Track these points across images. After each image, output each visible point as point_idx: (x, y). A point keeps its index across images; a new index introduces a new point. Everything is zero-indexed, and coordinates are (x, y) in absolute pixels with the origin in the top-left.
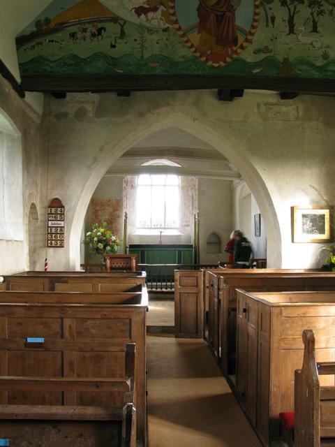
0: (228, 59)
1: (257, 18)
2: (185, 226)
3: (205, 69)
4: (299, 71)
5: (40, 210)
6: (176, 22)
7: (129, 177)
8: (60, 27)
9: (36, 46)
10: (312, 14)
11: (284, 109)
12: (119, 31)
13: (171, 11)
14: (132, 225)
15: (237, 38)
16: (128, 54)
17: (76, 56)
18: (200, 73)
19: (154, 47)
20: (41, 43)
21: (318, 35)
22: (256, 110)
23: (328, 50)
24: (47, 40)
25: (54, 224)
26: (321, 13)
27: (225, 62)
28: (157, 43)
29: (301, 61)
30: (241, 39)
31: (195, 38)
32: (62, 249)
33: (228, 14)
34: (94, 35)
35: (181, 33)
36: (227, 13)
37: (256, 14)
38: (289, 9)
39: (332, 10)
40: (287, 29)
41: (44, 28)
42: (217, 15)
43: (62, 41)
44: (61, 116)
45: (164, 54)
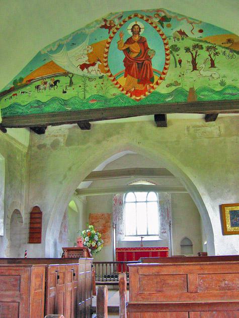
0: (147, 93)
1: (167, 62)
2: (163, 233)
3: (130, 102)
6: (109, 71)
8: (30, 82)
10: (210, 55)
11: (209, 129)
13: (105, 64)
14: (120, 234)
18: (126, 105)
19: (93, 90)
23: (224, 79)
26: (216, 54)
27: (145, 95)
29: (204, 89)
30: (156, 78)
31: (122, 81)
33: (146, 62)
34: (51, 86)
35: (112, 78)
36: (145, 62)
37: (167, 60)
38: (192, 54)
39: (225, 52)
40: (191, 68)
41: (19, 84)
42: (138, 64)
45: (100, 94)
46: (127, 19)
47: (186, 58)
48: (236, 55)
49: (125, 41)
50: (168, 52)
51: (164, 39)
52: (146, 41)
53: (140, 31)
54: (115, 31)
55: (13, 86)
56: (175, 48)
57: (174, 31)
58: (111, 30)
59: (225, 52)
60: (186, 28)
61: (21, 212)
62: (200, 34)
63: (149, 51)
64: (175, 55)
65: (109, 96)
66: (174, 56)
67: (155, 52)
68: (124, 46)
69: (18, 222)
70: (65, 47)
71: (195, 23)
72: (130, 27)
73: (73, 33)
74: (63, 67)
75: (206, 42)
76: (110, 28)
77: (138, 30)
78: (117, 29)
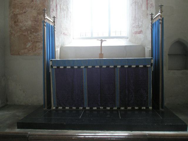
2: (136, 33)
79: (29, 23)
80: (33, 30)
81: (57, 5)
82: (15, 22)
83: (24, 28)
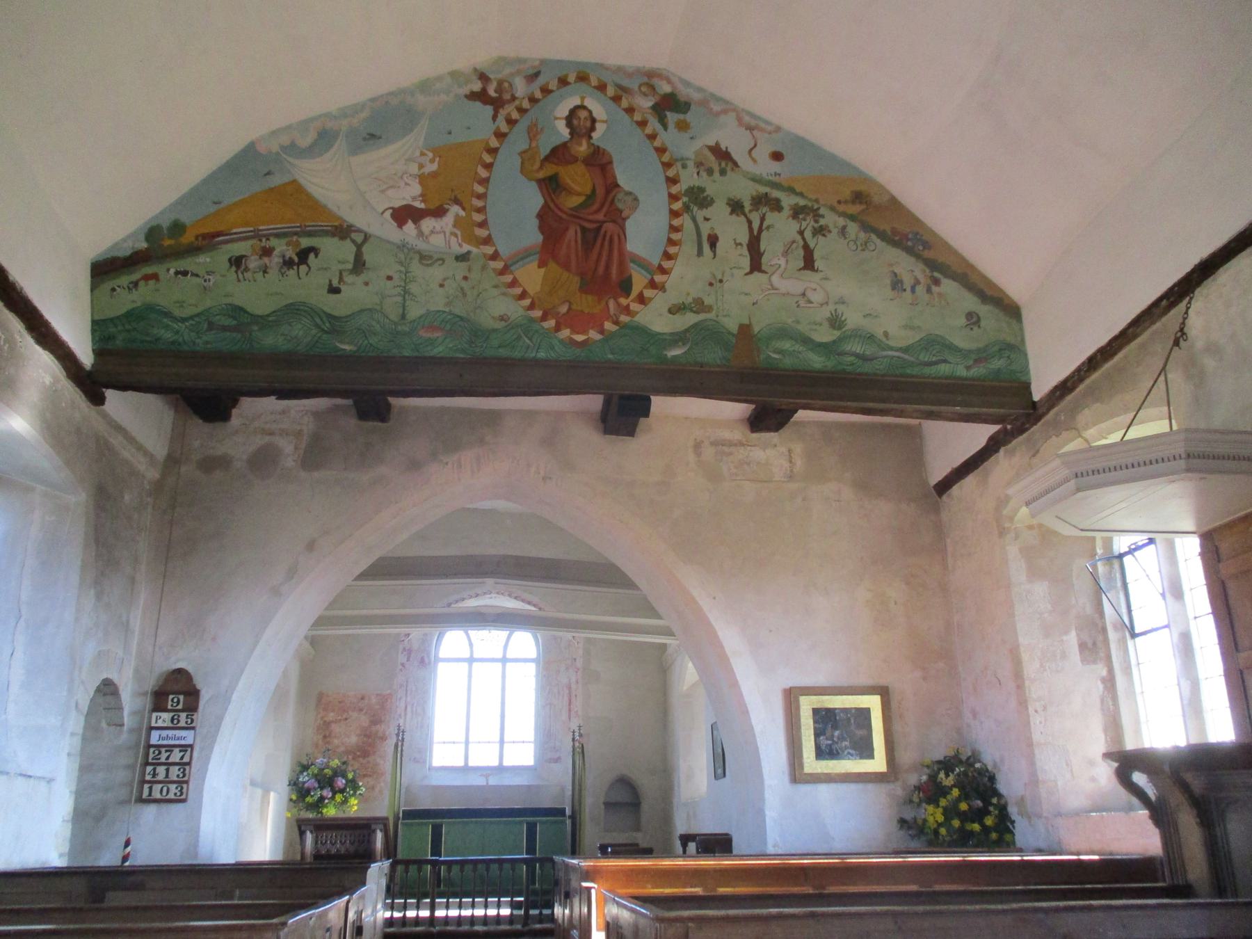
0: (608, 326)
1: (675, 236)
3: (552, 348)
4: (775, 352)
5: (131, 700)
6: (488, 241)
7: (416, 633)
8: (208, 241)
9: (142, 283)
10: (801, 233)
11: (758, 454)
12: (351, 258)
13: (478, 218)
14: (416, 761)
15: (630, 277)
16: (370, 310)
17: (241, 309)
20: (155, 277)
21: (815, 277)
22: (691, 457)
23: (841, 308)
24: (172, 271)
25: (168, 738)
26: (820, 231)
27: (602, 332)
28: (442, 286)
29: (783, 333)
30: (639, 280)
31: (532, 276)
32: (180, 805)
33: (609, 227)
34: (288, 263)
35: (499, 265)
36: (605, 225)
37: (675, 229)
38: (750, 222)
39: (844, 228)
40: (746, 262)
41: (167, 242)
42: (584, 229)
43: (208, 273)
44: (211, 464)
45: (457, 311)
46: (553, 85)
47: (733, 231)
48: (878, 241)
49: (545, 151)
50: (677, 206)
51: (667, 165)
52: (611, 162)
53: (593, 129)
54: (515, 115)
55: (144, 245)
56: (699, 198)
57: (698, 144)
58: (501, 111)
59: (844, 228)
60: (736, 142)
61: (121, 688)
62: (776, 167)
63: (620, 196)
64: (700, 219)
65: (486, 320)
66: (694, 220)
67: (636, 199)
68: (541, 167)
69: (104, 725)
70: (340, 145)
71: (762, 130)
72: (563, 110)
73: (373, 100)
74: (335, 209)
75: (791, 190)
76: (497, 104)
77: (588, 124)
78: (522, 111)
79: (353, 739)
80: (358, 753)
81: (406, 707)
82: (325, 737)
83: (342, 749)
